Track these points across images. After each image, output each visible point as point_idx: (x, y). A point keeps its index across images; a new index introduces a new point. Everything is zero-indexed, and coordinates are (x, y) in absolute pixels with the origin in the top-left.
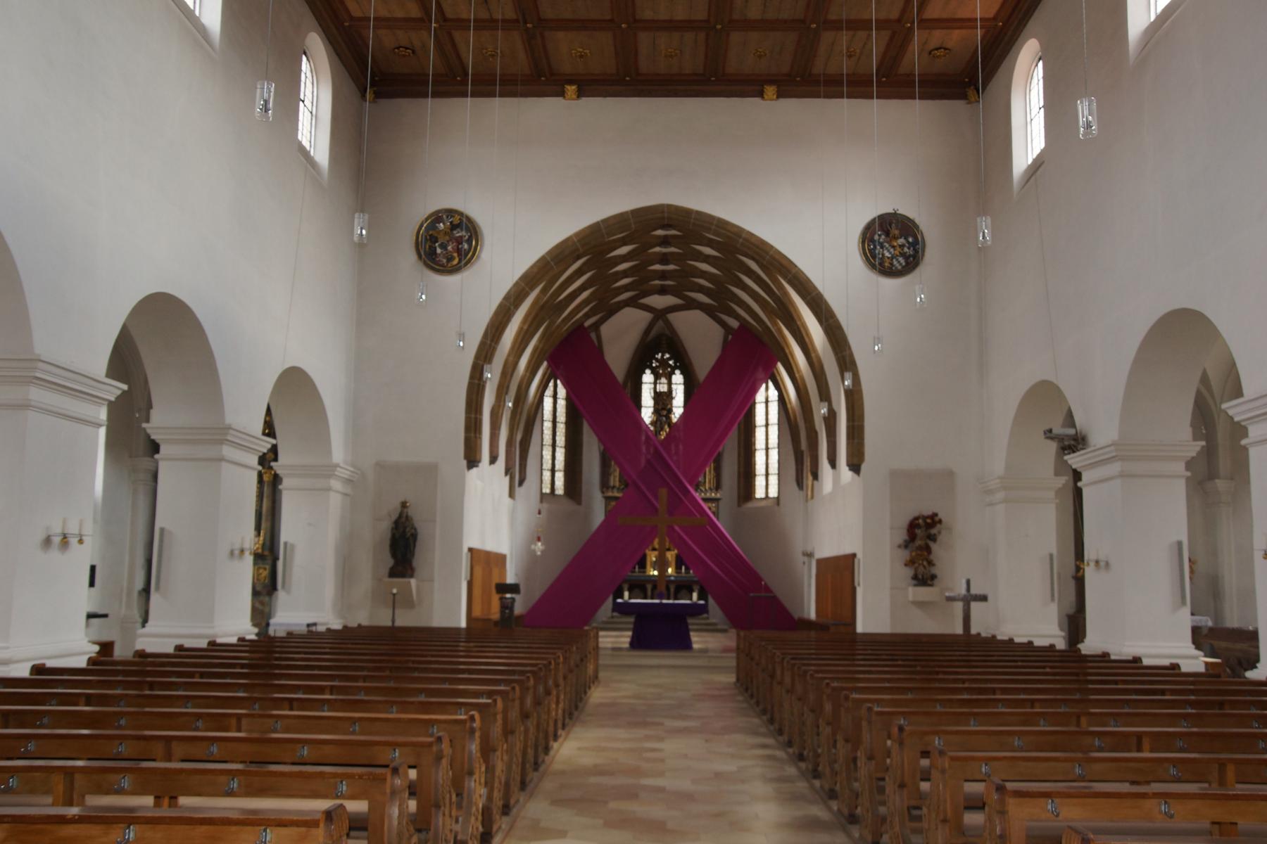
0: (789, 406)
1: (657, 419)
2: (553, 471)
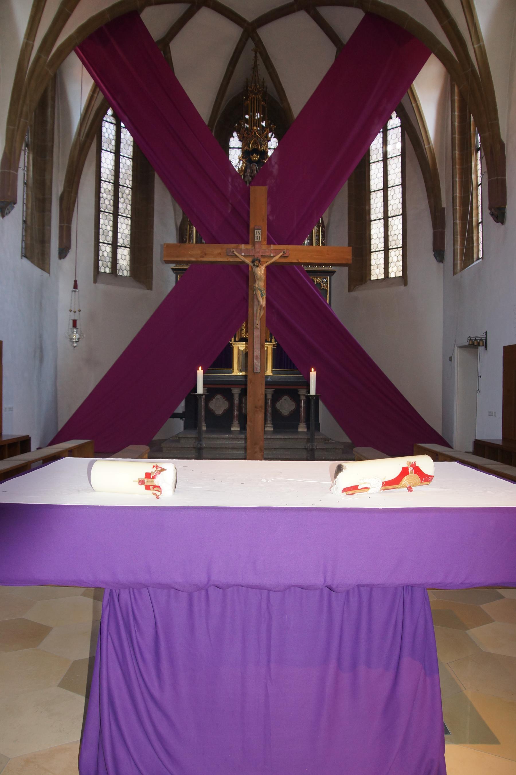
0: (427, 147)
1: (246, 168)
2: (115, 246)
